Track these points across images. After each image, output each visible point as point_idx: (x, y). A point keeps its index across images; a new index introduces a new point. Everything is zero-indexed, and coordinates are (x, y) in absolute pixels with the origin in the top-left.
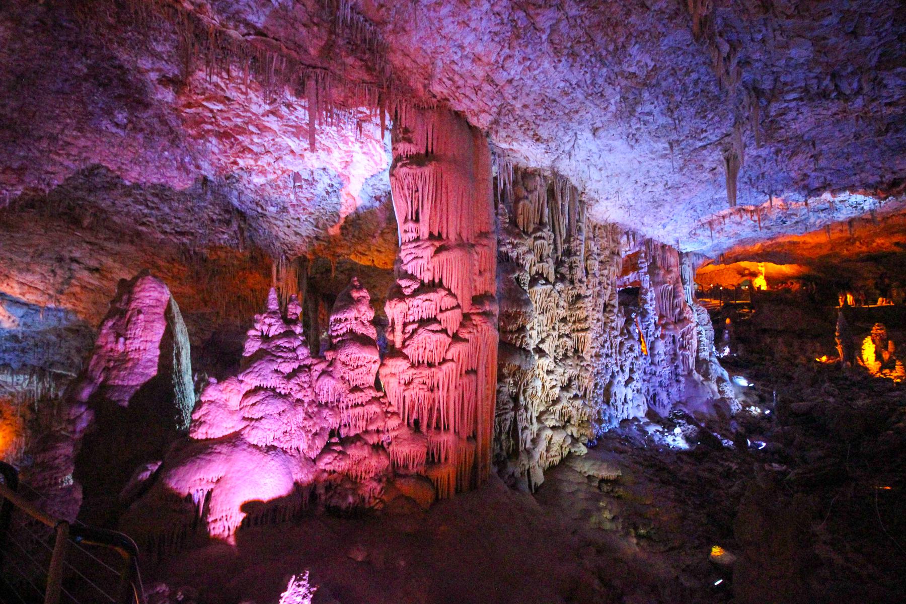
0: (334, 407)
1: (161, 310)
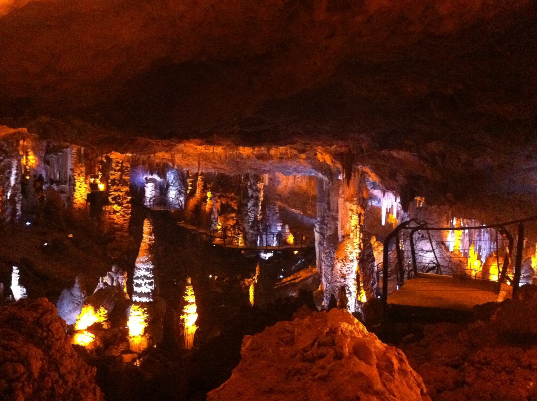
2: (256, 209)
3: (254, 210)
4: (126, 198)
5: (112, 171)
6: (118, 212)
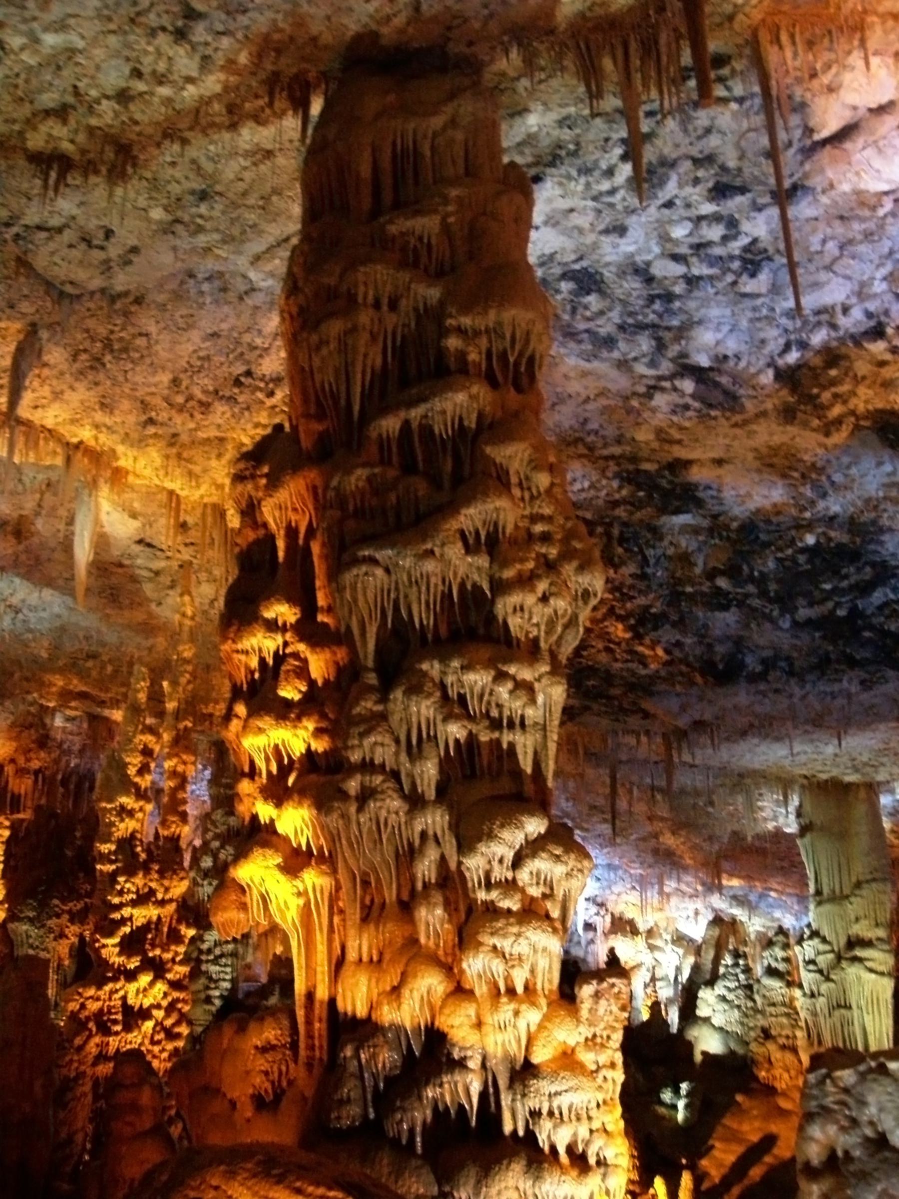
0: (762, 1012)
1: (713, 942)
2: (241, 951)
3: (234, 954)
4: (175, 937)
5: (127, 793)
6: (145, 1014)
